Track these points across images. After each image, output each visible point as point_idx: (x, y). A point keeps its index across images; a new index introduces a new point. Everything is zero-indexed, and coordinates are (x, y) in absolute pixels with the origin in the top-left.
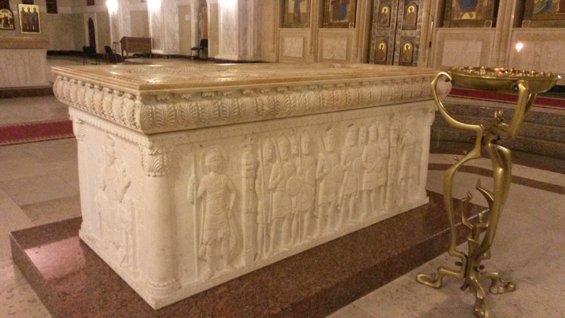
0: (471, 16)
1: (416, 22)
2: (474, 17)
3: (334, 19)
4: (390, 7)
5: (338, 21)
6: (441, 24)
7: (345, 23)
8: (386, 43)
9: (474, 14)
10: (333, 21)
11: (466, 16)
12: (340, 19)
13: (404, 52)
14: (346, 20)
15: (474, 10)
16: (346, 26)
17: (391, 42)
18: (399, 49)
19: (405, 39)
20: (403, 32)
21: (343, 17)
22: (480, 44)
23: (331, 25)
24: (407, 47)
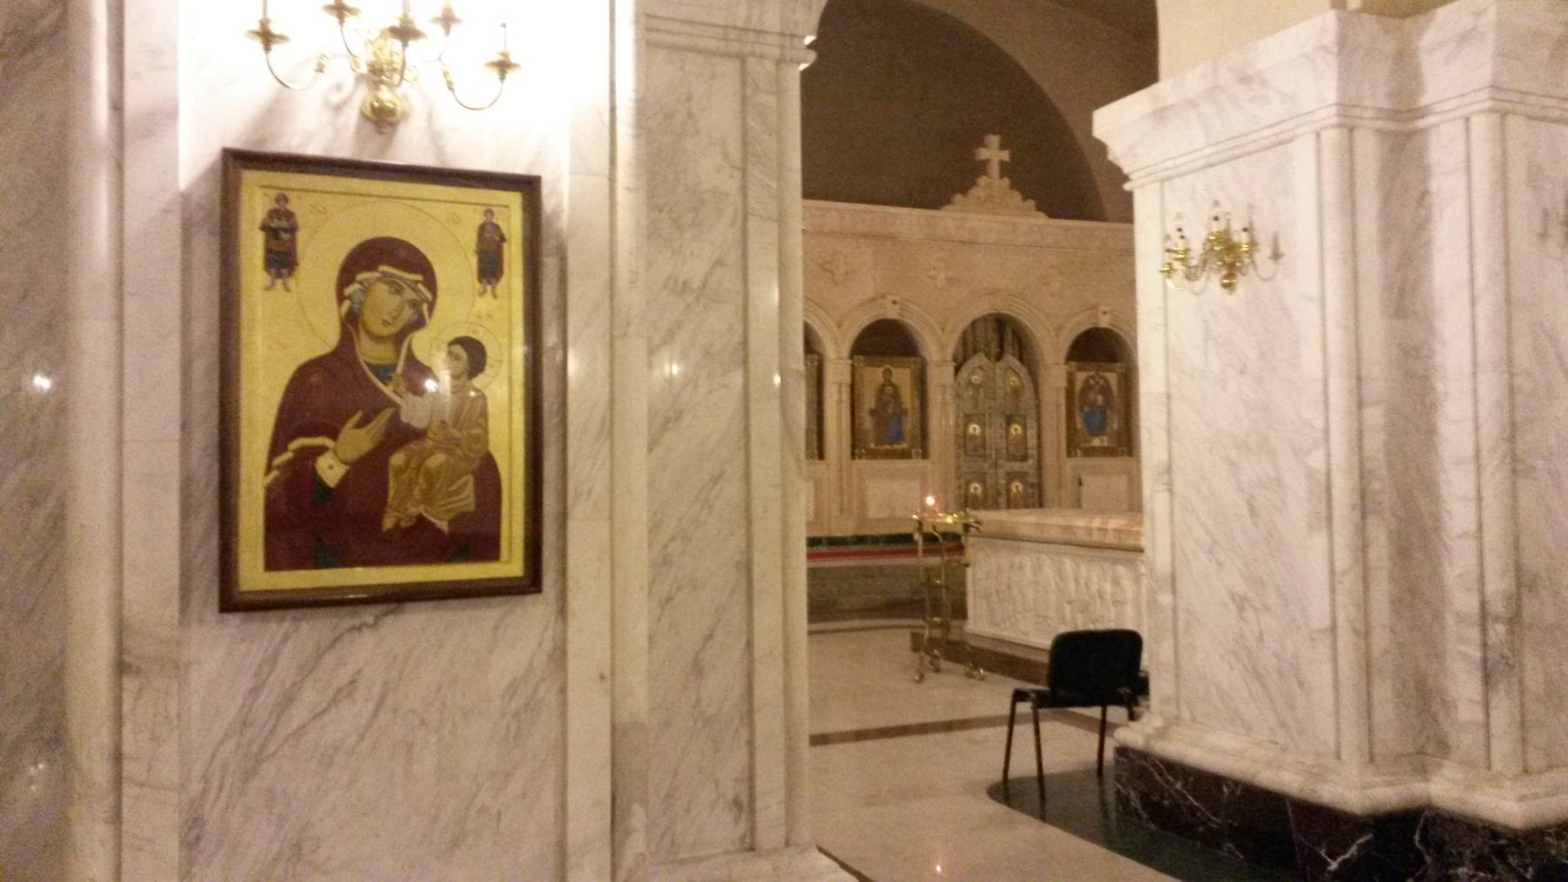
0: (1102, 441)
1: (1026, 449)
2: (1106, 444)
3: (879, 442)
4: (983, 425)
5: (887, 447)
6: (1070, 453)
7: (903, 450)
8: (983, 482)
9: (1105, 438)
10: (876, 445)
11: (1096, 442)
12: (891, 444)
13: (1012, 495)
14: (905, 445)
15: (1104, 434)
16: (905, 455)
17: (989, 481)
18: (1004, 492)
19: (1011, 477)
20: (1009, 464)
21: (899, 437)
22: (1124, 479)
23: (873, 455)
24: (1017, 487)
